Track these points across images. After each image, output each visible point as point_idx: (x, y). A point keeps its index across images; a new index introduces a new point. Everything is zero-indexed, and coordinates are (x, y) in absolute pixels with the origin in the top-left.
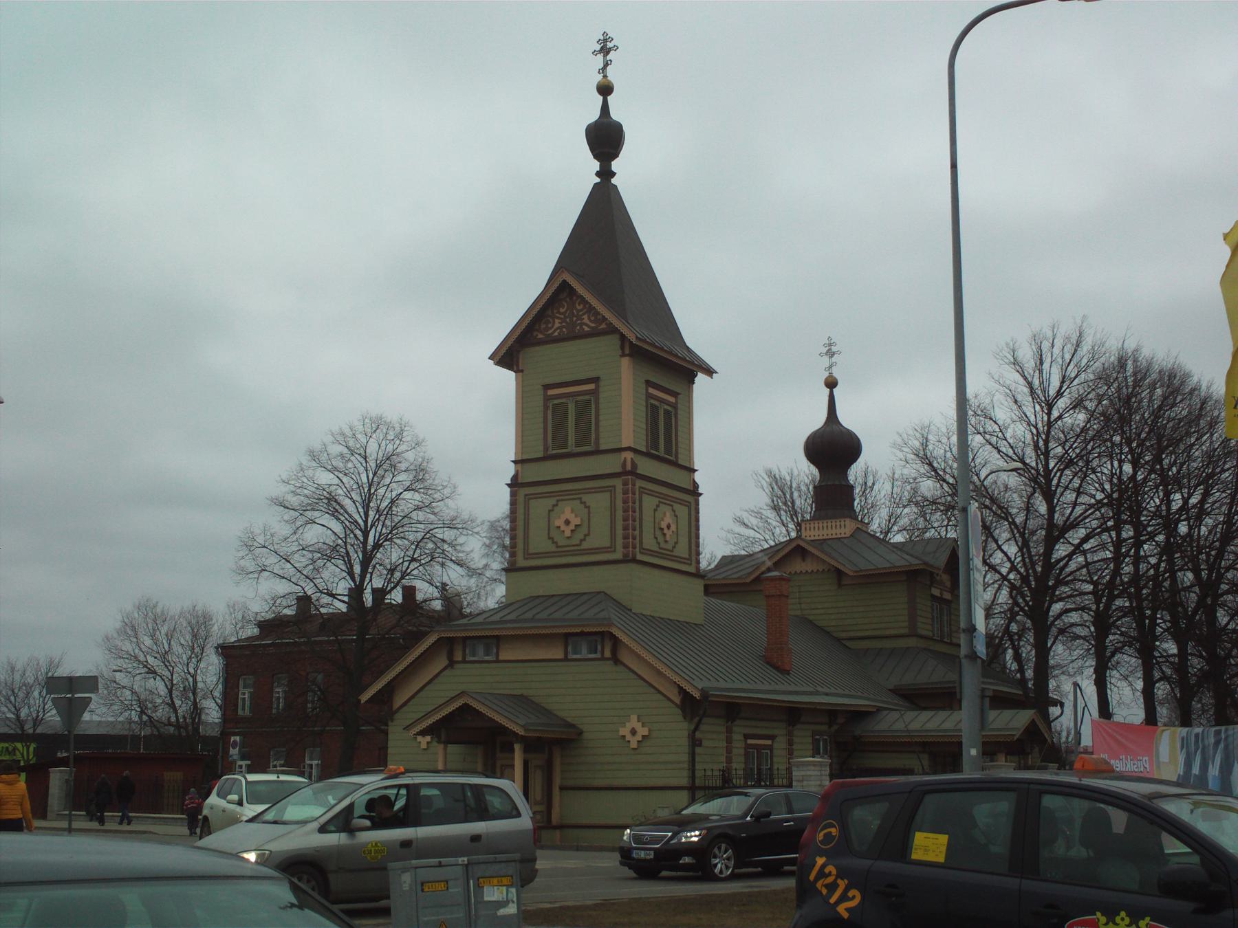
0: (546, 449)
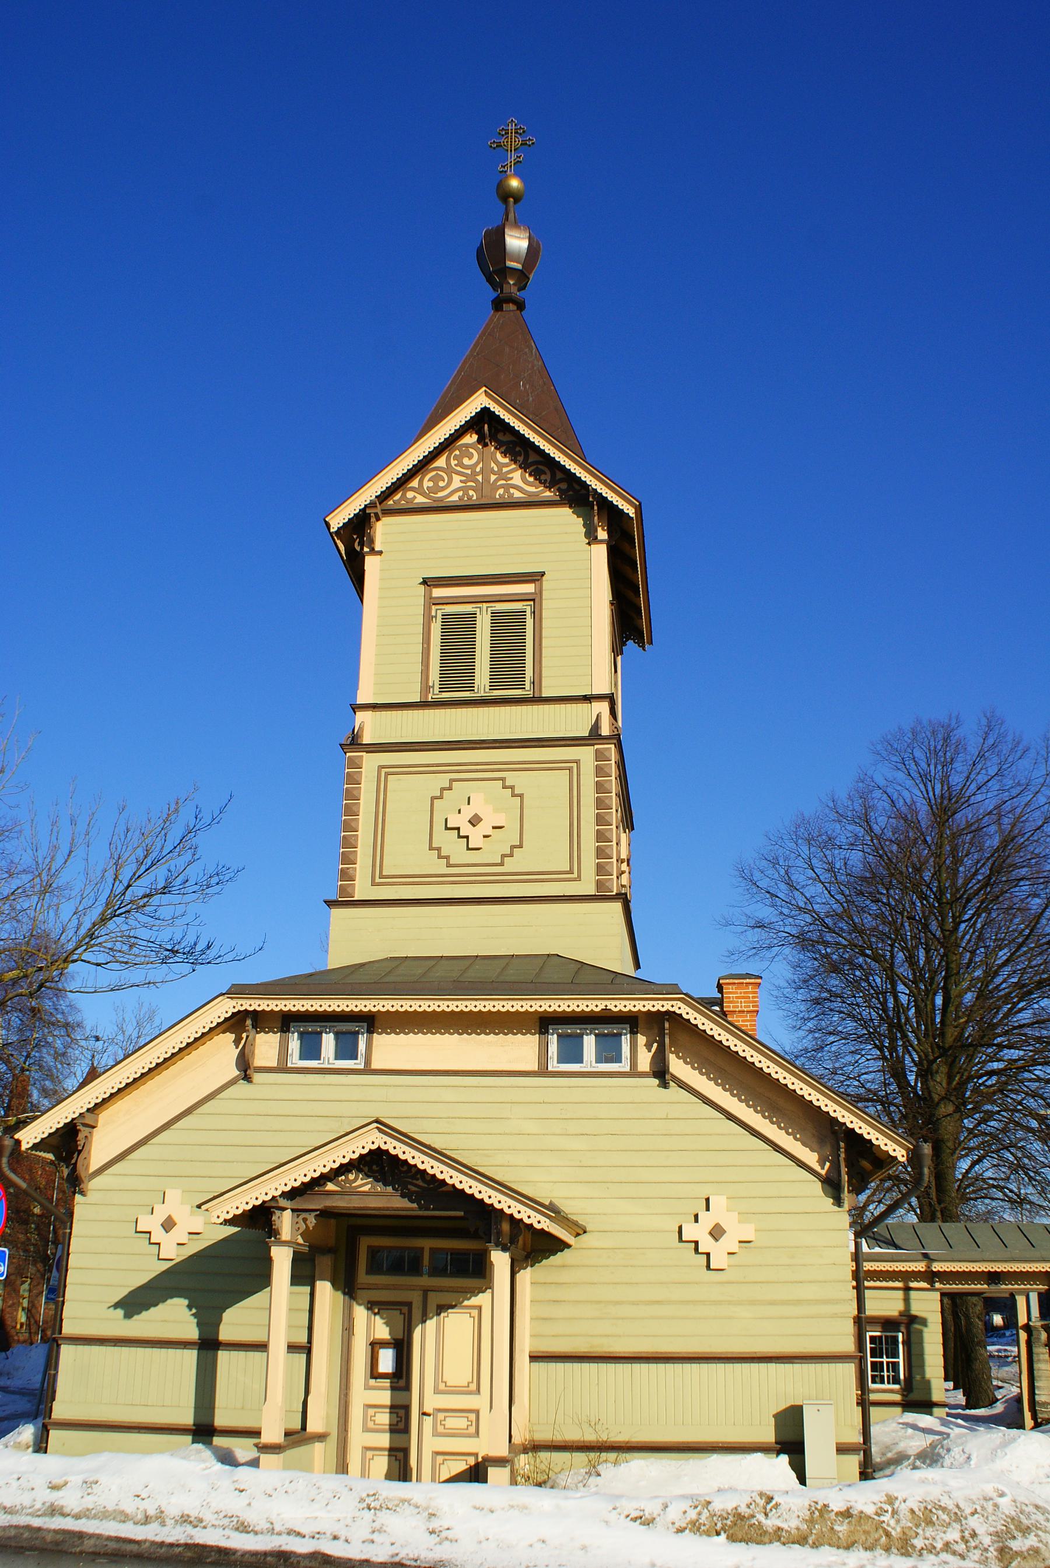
0: (426, 687)
